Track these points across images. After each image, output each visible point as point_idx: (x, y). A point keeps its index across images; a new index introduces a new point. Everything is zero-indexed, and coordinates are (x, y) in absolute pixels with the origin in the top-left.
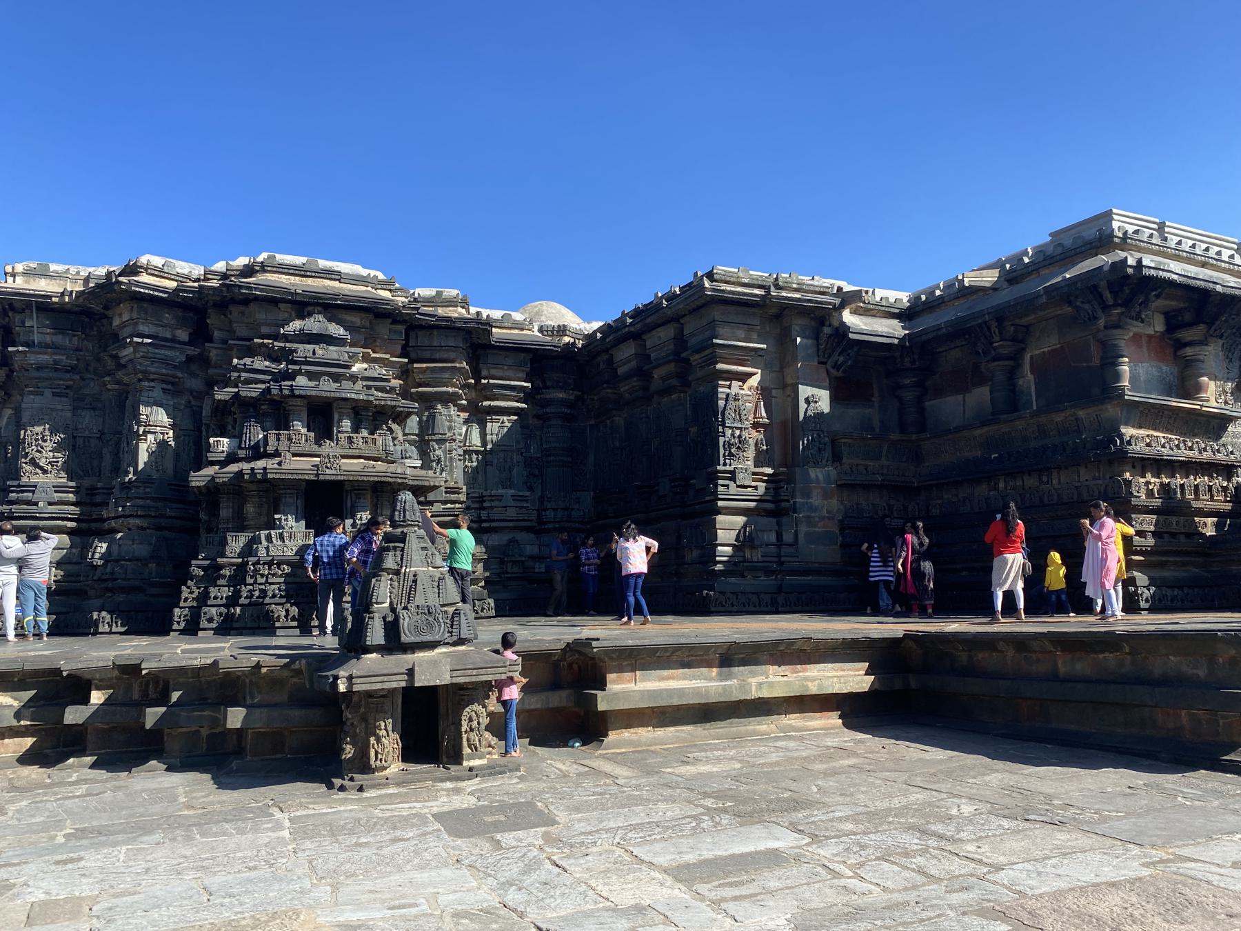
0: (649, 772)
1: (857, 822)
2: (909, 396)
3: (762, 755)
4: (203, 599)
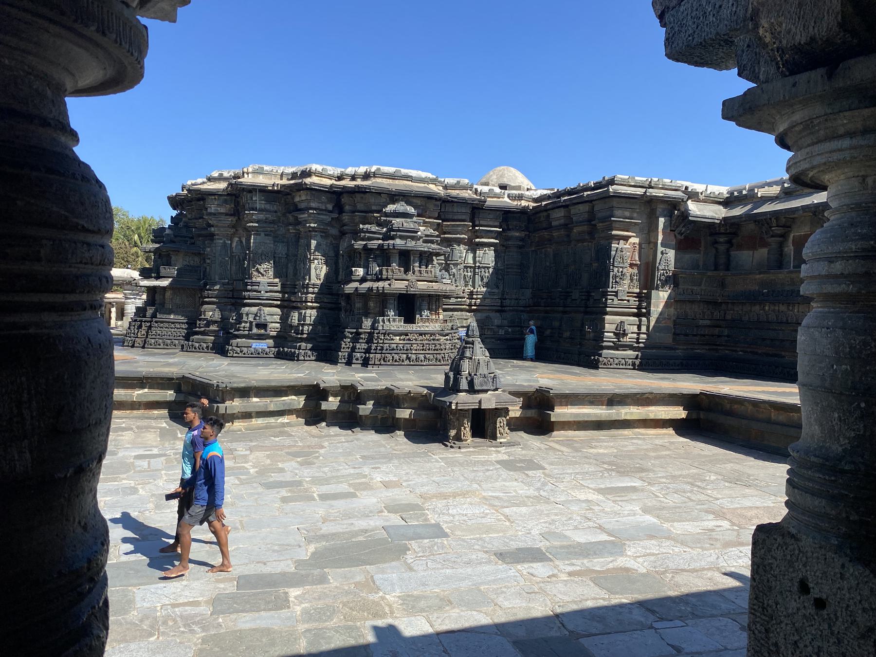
0: (577, 450)
2: (722, 248)
3: (626, 446)
4: (353, 349)
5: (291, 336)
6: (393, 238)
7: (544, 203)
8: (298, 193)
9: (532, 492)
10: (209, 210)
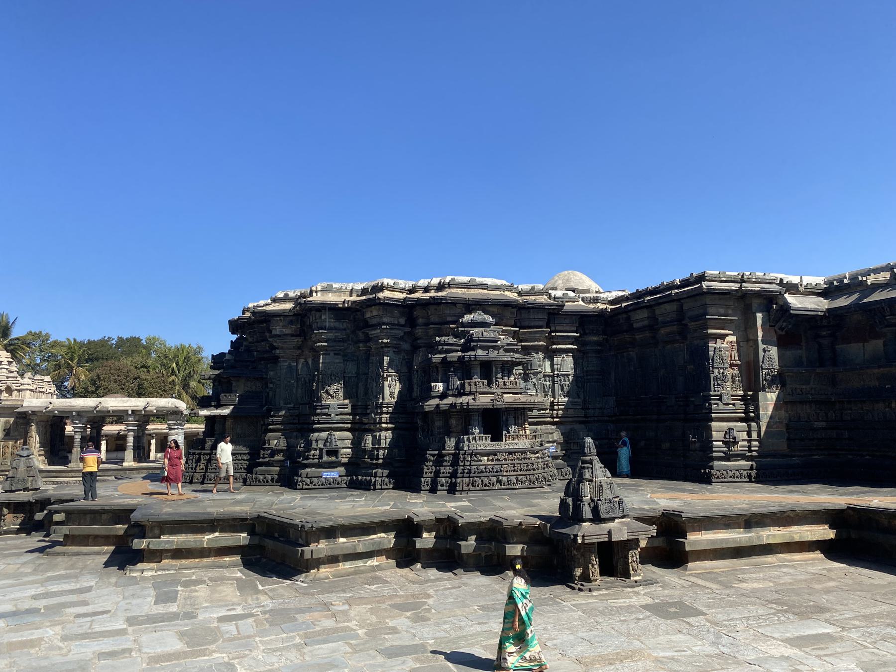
0: (727, 587)
1: (860, 621)
2: (825, 342)
4: (437, 474)
5: (365, 462)
6: (473, 349)
7: (624, 305)
8: (369, 309)
9: (709, 649)
10: (274, 332)
